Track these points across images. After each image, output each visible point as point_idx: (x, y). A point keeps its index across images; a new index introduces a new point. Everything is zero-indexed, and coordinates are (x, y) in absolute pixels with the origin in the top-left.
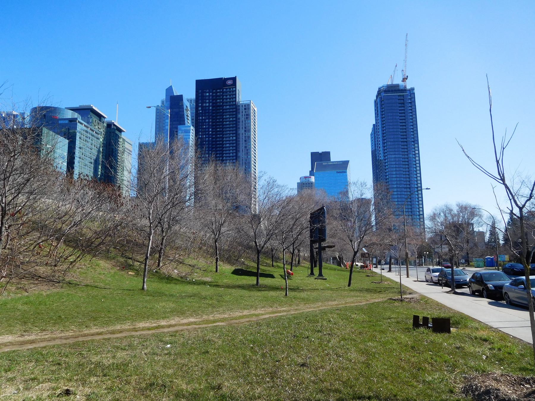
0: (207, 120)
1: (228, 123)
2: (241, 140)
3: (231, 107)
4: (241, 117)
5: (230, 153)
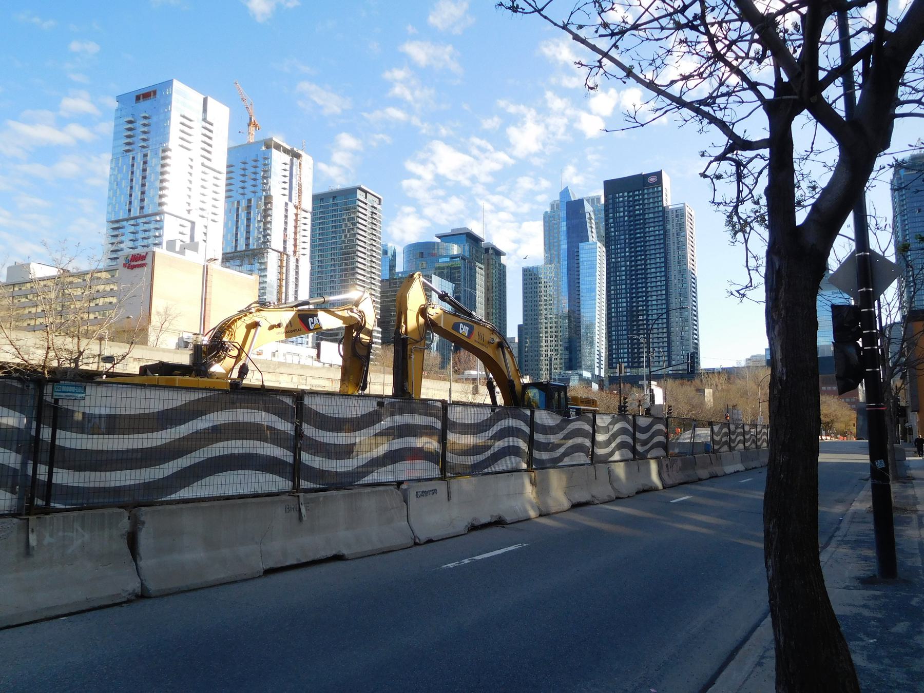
1: (652, 238)
3: (656, 215)
4: (672, 228)
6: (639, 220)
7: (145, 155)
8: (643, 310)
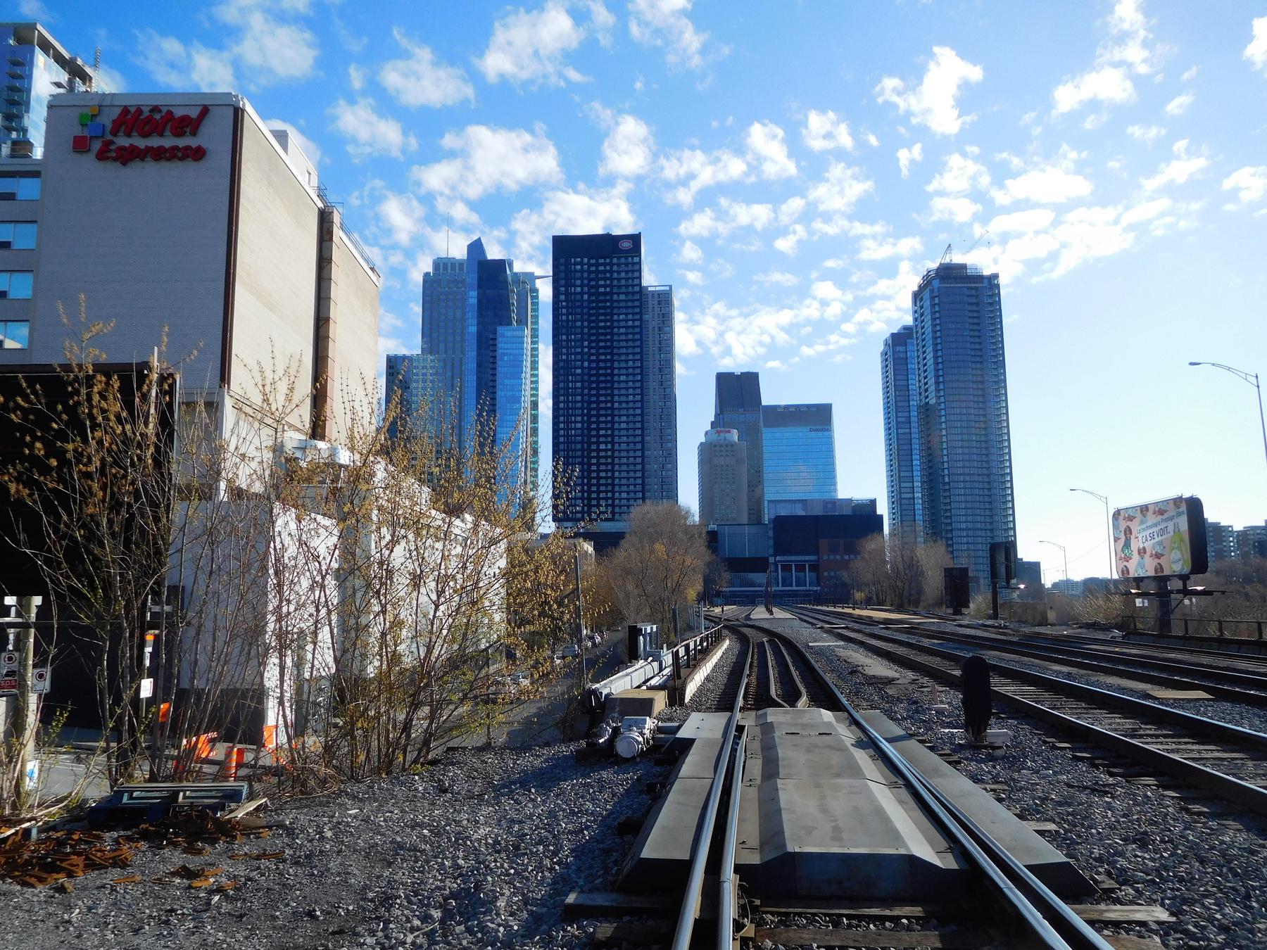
0: (579, 324)
1: (622, 330)
6: (606, 301)
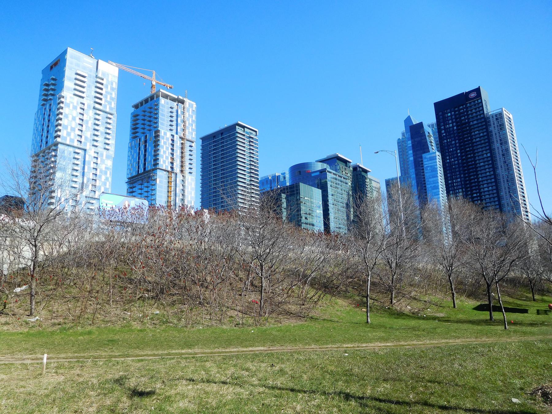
0: (453, 142)
1: (477, 140)
2: (497, 155)
3: (479, 121)
4: (493, 129)
5: (486, 173)
7: (50, 105)
8: (477, 197)
